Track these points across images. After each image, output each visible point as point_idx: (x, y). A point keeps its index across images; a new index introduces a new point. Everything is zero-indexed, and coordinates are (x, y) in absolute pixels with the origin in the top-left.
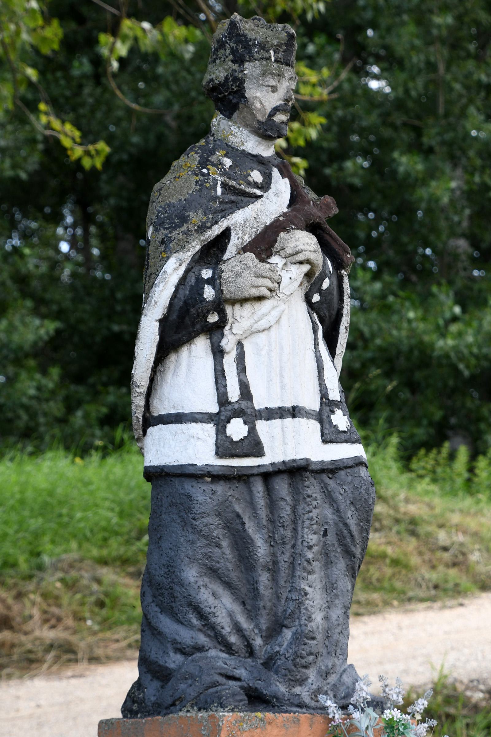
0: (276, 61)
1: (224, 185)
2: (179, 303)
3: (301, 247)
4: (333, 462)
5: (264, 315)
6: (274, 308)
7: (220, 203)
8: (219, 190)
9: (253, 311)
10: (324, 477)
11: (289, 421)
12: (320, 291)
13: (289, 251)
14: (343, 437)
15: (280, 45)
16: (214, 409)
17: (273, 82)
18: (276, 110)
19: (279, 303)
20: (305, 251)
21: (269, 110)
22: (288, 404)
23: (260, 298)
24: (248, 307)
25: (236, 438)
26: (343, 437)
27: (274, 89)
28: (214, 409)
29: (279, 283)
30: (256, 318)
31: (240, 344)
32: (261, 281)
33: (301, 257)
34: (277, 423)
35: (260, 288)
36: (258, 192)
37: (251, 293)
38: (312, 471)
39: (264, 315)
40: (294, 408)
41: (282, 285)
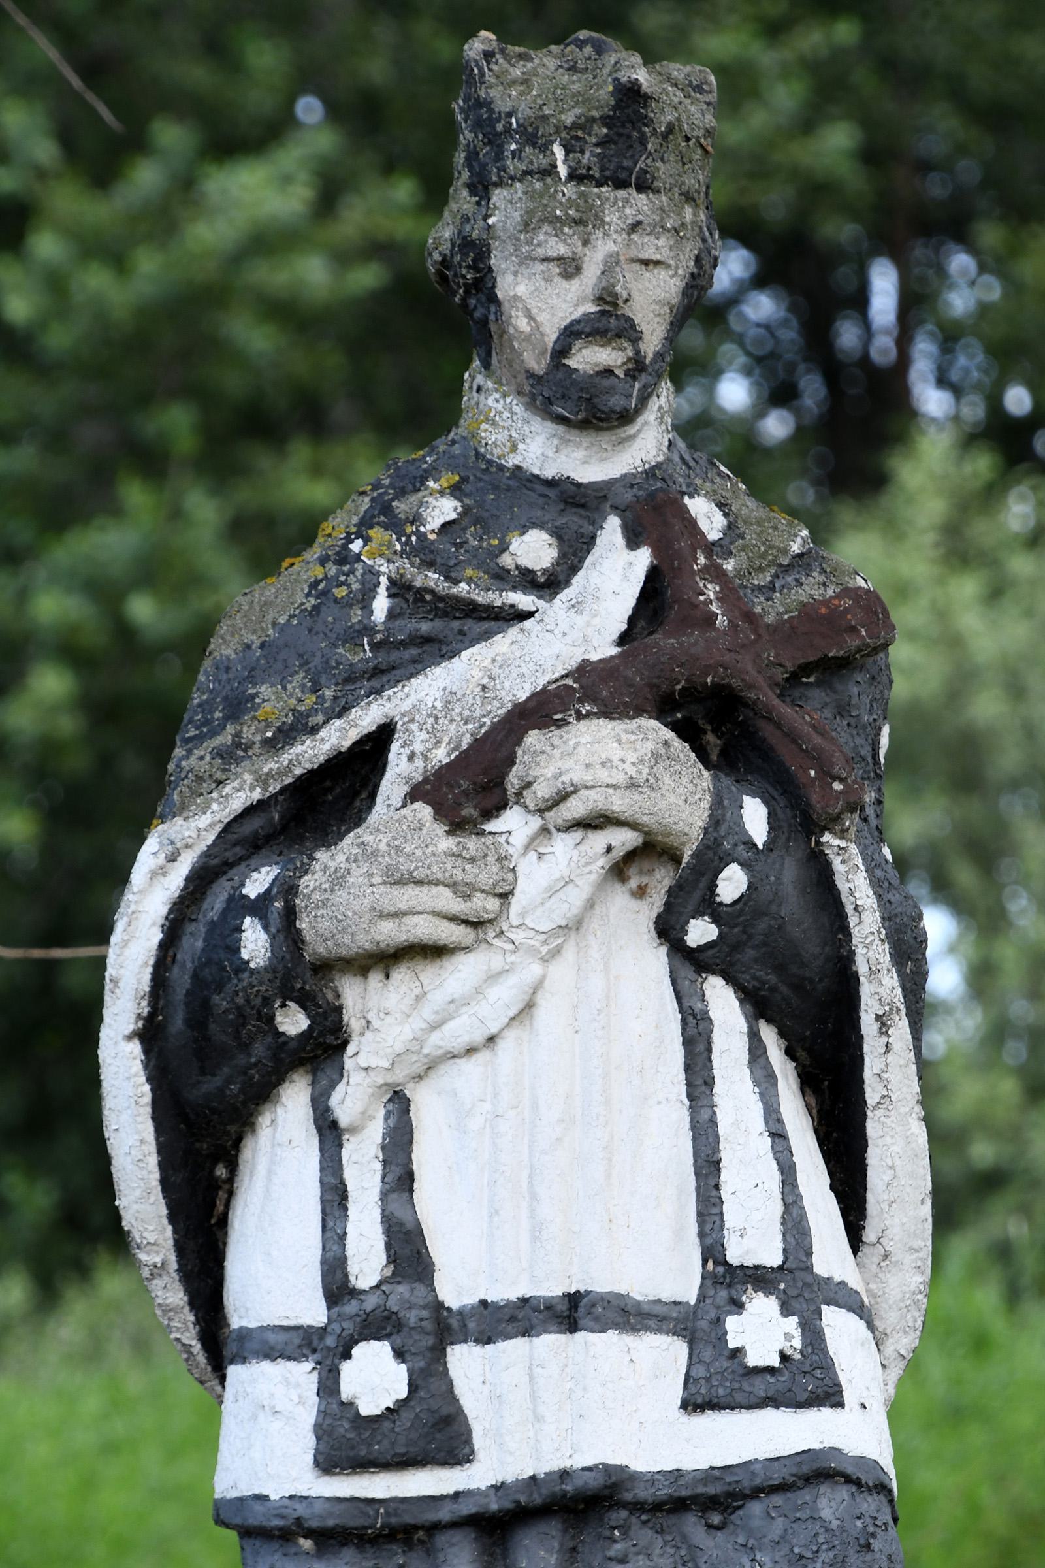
0: (571, 177)
1: (399, 588)
2: (181, 979)
3: (576, 775)
4: (714, 1474)
5: (456, 1005)
6: (493, 977)
7: (375, 647)
8: (381, 605)
9: (418, 991)
10: (692, 1525)
11: (550, 1343)
12: (710, 907)
13: (542, 791)
14: (760, 1386)
15: (583, 125)
16: (315, 1313)
17: (558, 248)
18: (572, 334)
19: (511, 958)
20: (587, 788)
21: (551, 336)
22: (553, 1288)
23: (435, 952)
24: (401, 975)
25: (368, 1408)
26: (760, 1386)
27: (570, 268)
28: (315, 1313)
29: (505, 896)
30: (427, 1012)
31: (399, 1102)
32: (407, 897)
33: (575, 808)
34: (513, 1349)
35: (409, 920)
36: (522, 600)
37: (378, 938)
38: (637, 1507)
39: (456, 1005)
40: (574, 1299)
41: (517, 903)
